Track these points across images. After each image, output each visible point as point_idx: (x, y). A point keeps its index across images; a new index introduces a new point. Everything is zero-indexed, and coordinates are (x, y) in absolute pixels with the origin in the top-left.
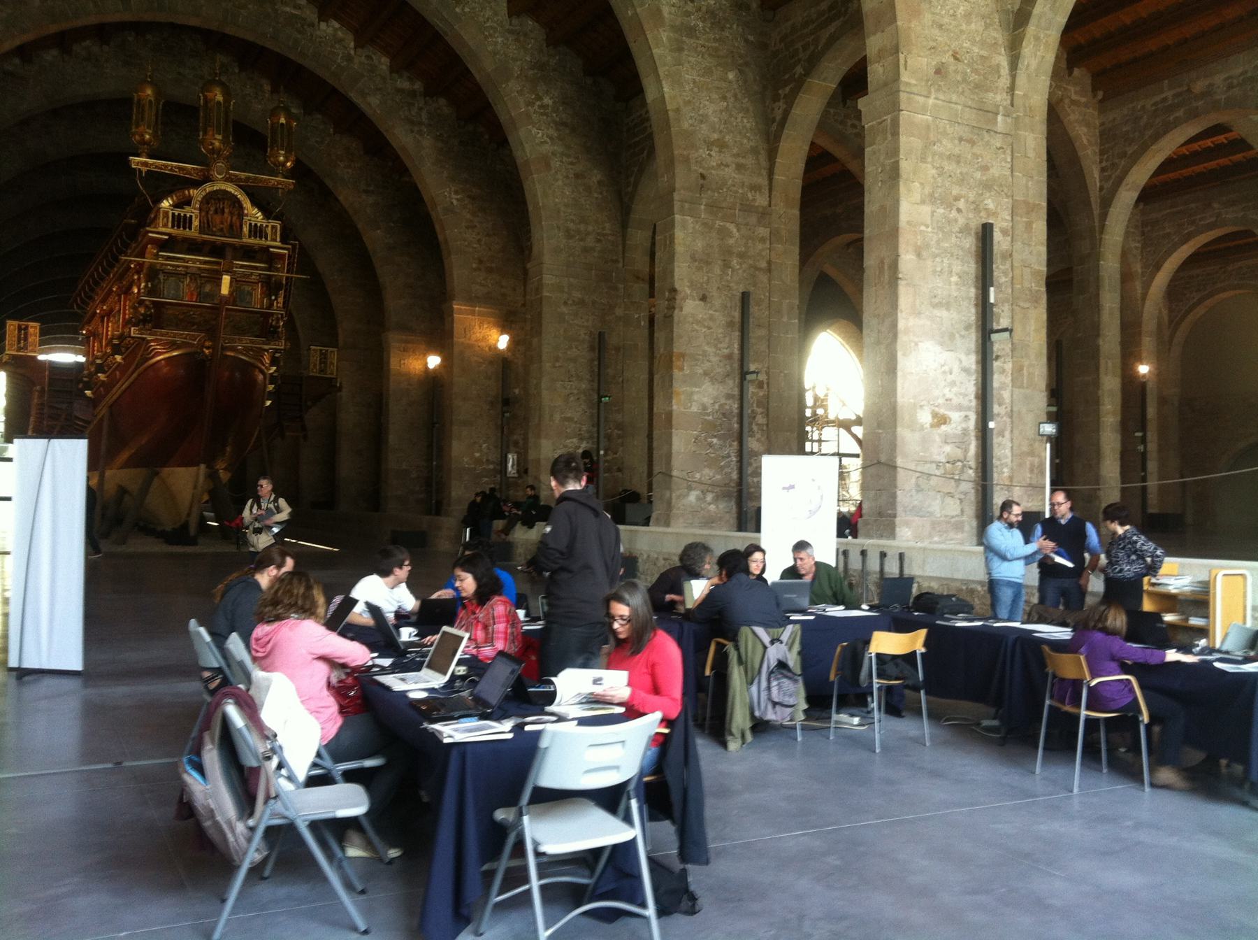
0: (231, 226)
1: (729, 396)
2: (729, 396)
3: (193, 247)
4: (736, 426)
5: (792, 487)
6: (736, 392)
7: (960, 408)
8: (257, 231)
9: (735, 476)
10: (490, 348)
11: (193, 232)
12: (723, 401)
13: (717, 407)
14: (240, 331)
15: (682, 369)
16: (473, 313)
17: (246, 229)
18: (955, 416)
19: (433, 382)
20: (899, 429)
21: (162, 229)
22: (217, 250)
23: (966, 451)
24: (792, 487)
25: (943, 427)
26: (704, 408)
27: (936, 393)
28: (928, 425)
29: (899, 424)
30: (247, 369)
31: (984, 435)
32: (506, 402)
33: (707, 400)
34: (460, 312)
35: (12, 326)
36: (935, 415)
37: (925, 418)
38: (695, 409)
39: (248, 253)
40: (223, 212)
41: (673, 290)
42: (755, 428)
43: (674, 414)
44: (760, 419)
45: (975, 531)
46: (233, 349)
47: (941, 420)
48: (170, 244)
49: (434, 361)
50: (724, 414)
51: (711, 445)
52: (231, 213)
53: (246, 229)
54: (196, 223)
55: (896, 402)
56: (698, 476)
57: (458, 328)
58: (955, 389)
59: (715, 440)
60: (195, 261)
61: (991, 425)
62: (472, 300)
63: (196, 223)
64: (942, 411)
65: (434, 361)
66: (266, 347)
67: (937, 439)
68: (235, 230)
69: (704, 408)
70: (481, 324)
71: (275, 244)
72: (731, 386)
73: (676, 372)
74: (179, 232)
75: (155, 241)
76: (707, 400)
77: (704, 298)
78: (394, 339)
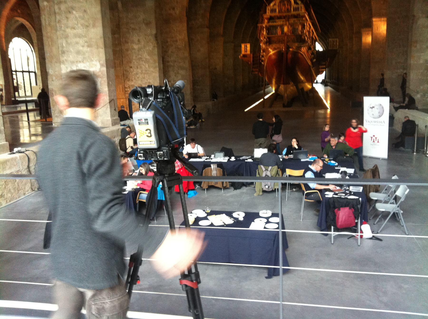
0: (288, 9)
3: (279, 18)
5: (373, 107)
8: (296, 9)
11: (277, 13)
14: (294, 42)
15: (416, 47)
16: (381, 21)
21: (268, 14)
22: (284, 17)
24: (373, 107)
34: (376, 21)
35: (243, 46)
38: (421, 62)
40: (285, 5)
41: (414, 16)
46: (292, 48)
48: (271, 19)
52: (288, 5)
54: (277, 10)
56: (422, 87)
60: (279, 22)
63: (277, 10)
66: (302, 45)
68: (288, 10)
71: (303, 11)
74: (273, 14)
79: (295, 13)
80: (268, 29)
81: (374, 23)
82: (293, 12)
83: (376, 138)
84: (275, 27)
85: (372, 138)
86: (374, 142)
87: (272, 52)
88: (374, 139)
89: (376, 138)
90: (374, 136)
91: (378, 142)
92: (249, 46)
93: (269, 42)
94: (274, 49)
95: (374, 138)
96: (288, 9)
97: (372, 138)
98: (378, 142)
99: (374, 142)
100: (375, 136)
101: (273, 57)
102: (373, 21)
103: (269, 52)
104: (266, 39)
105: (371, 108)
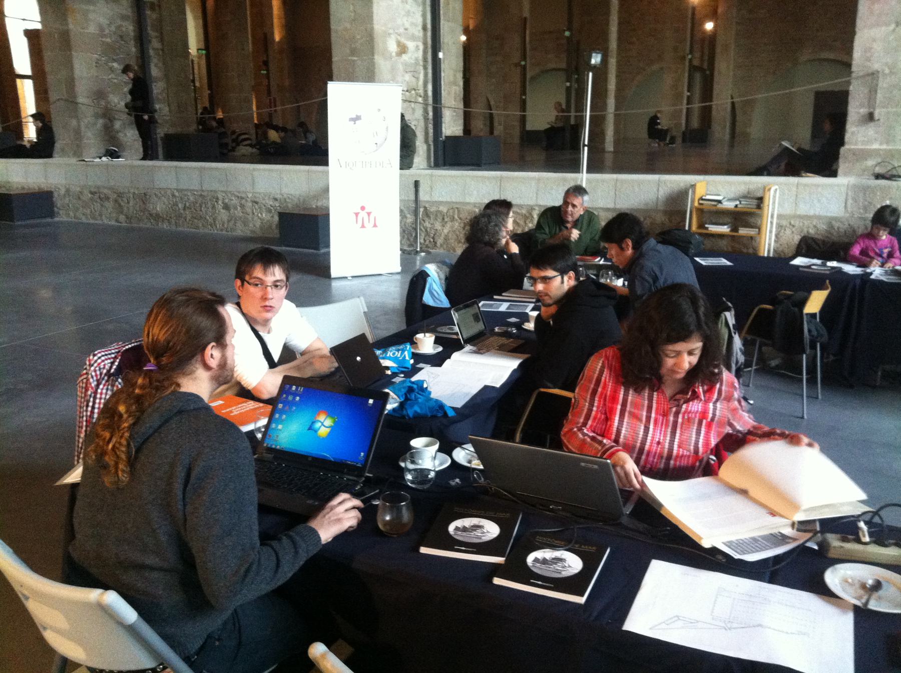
1: (124, 18)
2: (124, 18)
4: (134, 49)
7: (413, 38)
12: (119, 22)
13: (113, 28)
18: (411, 45)
20: (376, 57)
23: (418, 79)
25: (405, 57)
26: (102, 29)
27: (399, 22)
28: (394, 54)
29: (376, 51)
31: (436, 64)
33: (104, 21)
36: (399, 44)
37: (393, 47)
42: (151, 52)
43: (72, 34)
45: (425, 155)
47: (403, 50)
50: (121, 37)
51: (112, 69)
55: (372, 29)
58: (410, 20)
59: (115, 65)
61: (441, 55)
64: (403, 40)
67: (401, 67)
76: (104, 21)
83: (369, 214)
85: (357, 214)
86: (363, 226)
88: (364, 216)
89: (369, 214)
90: (363, 208)
91: (375, 226)
95: (363, 214)
97: (357, 214)
98: (375, 226)
99: (363, 226)
100: (367, 210)
105: (352, 119)
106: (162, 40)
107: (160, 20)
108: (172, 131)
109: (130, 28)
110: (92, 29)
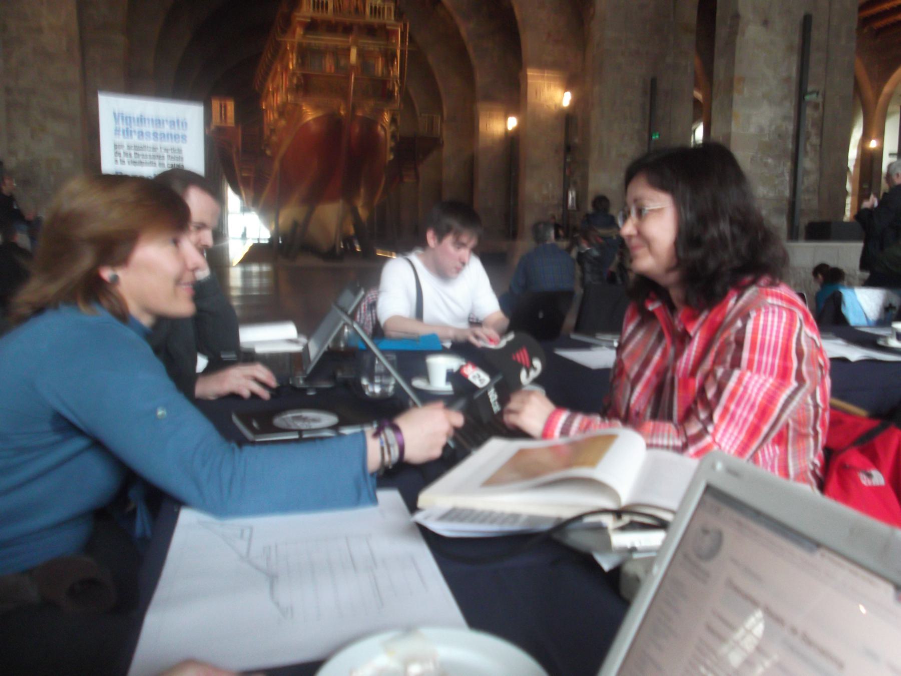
0: (357, 9)
2: (785, 118)
6: (792, 113)
8: (375, 11)
9: (787, 193)
10: (556, 106)
13: (773, 127)
17: (368, 10)
19: (512, 141)
26: (761, 129)
30: (370, 125)
32: (569, 149)
39: (371, 31)
42: (809, 148)
44: (815, 140)
48: (312, 26)
49: (512, 123)
50: (779, 135)
51: (766, 165)
53: (368, 10)
54: (331, 6)
57: (531, 91)
59: (770, 161)
62: (543, 66)
65: (512, 123)
69: (761, 129)
70: (549, 86)
72: (789, 108)
73: (736, 96)
74: (319, 15)
75: (301, 23)
77: (765, 23)
78: (482, 109)
79: (375, 21)
80: (304, 53)
81: (529, 81)
82: (369, 18)
84: (320, 53)
87: (310, 115)
92: (231, 106)
93: (305, 86)
94: (316, 107)
96: (357, 9)
101: (314, 128)
102: (526, 75)
103: (301, 115)
104: (299, 79)
106: (821, 134)
107: (822, 118)
108: (816, 218)
109: (790, 127)
110: (752, 130)
